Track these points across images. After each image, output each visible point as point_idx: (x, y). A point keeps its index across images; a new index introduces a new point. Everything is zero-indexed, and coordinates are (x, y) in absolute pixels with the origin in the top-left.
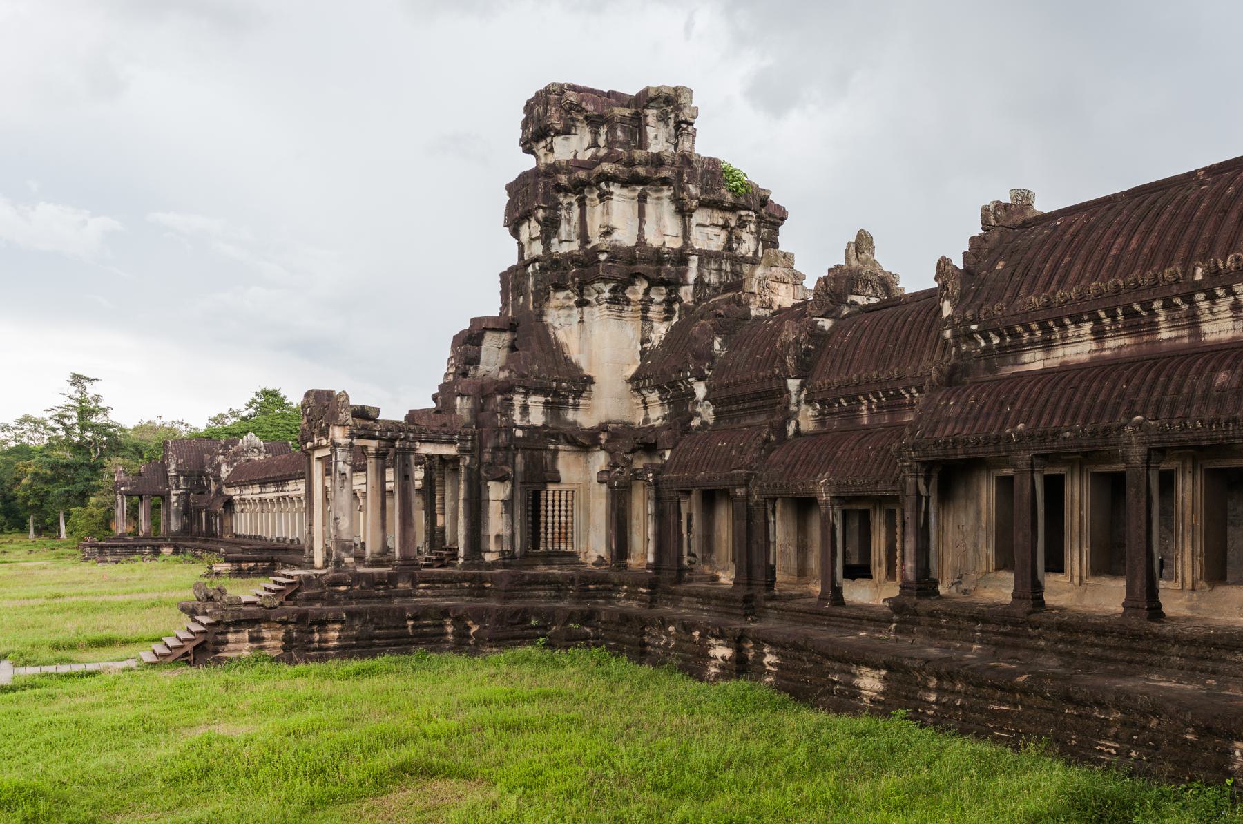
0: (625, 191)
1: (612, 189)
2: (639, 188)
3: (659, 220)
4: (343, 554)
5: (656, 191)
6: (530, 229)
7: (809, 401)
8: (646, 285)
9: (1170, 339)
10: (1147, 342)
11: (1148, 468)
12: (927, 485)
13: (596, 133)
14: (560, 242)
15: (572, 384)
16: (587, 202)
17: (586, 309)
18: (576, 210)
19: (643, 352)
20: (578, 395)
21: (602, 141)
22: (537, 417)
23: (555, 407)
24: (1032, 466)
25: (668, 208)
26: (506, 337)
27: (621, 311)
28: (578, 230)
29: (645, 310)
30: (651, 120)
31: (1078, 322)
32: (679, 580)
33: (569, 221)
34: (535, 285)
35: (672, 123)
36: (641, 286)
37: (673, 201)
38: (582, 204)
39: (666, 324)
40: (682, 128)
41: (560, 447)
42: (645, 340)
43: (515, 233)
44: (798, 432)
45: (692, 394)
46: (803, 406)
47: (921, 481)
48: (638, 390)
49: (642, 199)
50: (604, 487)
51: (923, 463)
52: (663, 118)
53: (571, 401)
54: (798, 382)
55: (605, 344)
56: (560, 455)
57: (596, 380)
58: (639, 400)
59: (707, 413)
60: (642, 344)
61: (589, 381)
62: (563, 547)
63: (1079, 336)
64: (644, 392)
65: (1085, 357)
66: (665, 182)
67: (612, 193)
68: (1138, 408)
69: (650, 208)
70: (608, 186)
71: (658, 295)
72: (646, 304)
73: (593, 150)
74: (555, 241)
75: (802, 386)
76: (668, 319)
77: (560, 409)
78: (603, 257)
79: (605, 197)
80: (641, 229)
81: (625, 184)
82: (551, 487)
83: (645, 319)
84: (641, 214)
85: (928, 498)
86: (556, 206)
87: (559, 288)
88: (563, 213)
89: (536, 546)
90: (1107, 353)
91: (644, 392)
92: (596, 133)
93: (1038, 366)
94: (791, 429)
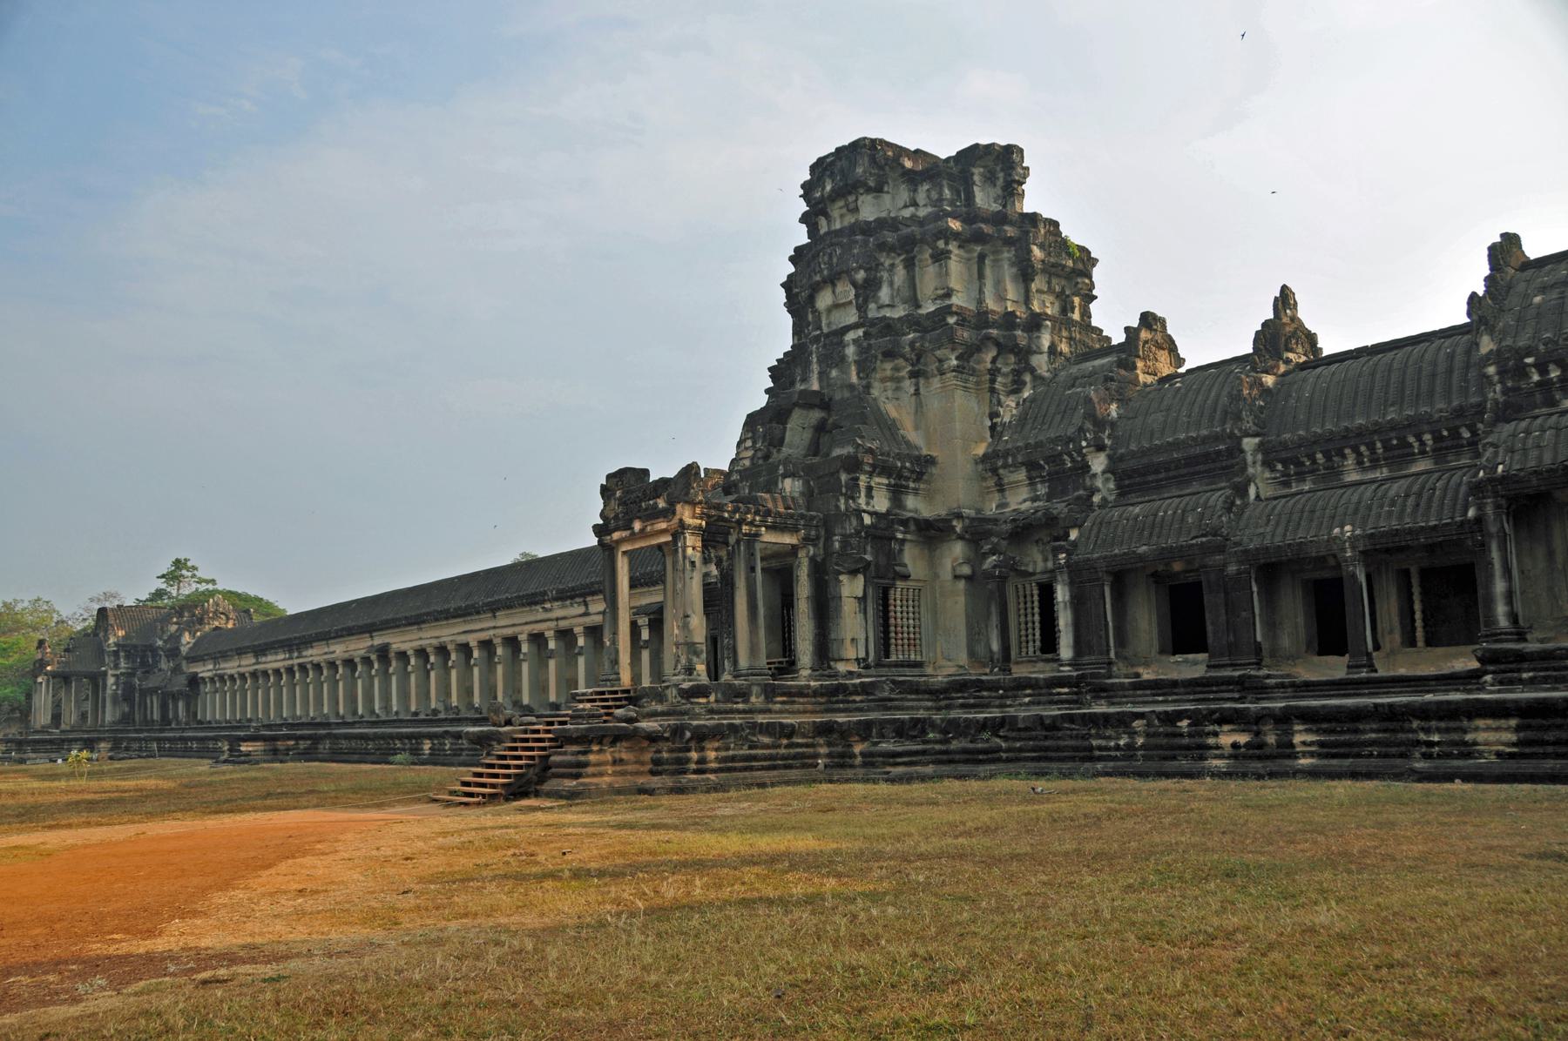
0: (961, 252)
1: (950, 247)
2: (979, 249)
3: (998, 283)
4: (695, 659)
5: (994, 253)
8: (992, 353)
14: (881, 307)
15: (911, 470)
17: (922, 381)
19: (993, 428)
20: (919, 477)
21: (921, 197)
23: (897, 493)
25: (1008, 272)
26: (816, 415)
27: (966, 381)
28: (906, 293)
29: (993, 381)
30: (976, 178)
33: (891, 284)
35: (1000, 182)
36: (989, 355)
37: (1012, 265)
38: (910, 264)
39: (1012, 397)
41: (909, 537)
42: (993, 415)
48: (994, 471)
49: (982, 258)
50: (961, 584)
52: (990, 179)
55: (948, 422)
56: (907, 547)
57: (940, 460)
58: (991, 483)
61: (931, 461)
64: (1001, 471)
66: (1009, 242)
67: (950, 252)
69: (988, 272)
70: (947, 244)
71: (1008, 364)
72: (994, 373)
73: (912, 209)
74: (872, 306)
78: (951, 320)
79: (940, 257)
80: (981, 291)
81: (964, 241)
82: (900, 584)
83: (993, 391)
84: (981, 276)
86: (873, 267)
87: (889, 355)
88: (885, 275)
89: (887, 656)
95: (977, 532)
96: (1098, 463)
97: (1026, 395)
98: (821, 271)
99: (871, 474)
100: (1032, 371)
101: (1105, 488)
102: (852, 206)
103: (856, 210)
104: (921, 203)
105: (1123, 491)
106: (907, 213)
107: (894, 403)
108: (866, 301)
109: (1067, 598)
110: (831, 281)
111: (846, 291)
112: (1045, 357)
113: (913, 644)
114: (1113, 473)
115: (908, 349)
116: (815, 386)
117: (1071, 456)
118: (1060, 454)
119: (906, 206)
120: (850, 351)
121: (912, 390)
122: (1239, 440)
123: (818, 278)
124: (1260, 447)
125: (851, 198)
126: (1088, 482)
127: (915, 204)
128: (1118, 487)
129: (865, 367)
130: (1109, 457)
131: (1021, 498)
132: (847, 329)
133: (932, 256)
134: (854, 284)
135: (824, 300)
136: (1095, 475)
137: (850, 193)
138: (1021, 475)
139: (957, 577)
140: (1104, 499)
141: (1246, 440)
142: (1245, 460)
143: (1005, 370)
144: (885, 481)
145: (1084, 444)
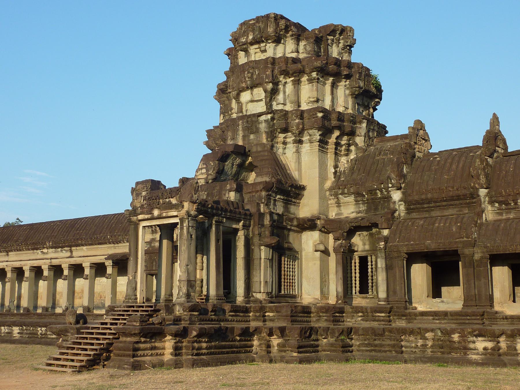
57: (308, 188)
60: (335, 169)
61: (303, 188)
71: (344, 141)
73: (296, 54)
74: (274, 103)
77: (289, 204)
86: (276, 84)
91: (340, 196)
95: (328, 227)
96: (396, 196)
97: (352, 156)
98: (246, 82)
99: (276, 193)
100: (356, 145)
101: (401, 209)
102: (263, 49)
103: (265, 51)
104: (301, 51)
105: (409, 210)
106: (294, 55)
107: (288, 155)
108: (271, 100)
109: (384, 266)
110: (252, 87)
111: (259, 93)
112: (362, 138)
113: (291, 285)
114: (405, 202)
115: (295, 128)
116: (240, 143)
117: (381, 192)
118: (376, 190)
119: (292, 52)
120: (263, 127)
121: (294, 150)
122: (477, 189)
123: (244, 85)
124: (488, 194)
125: (263, 45)
126: (392, 206)
127: (298, 52)
128: (407, 209)
129: (272, 135)
130: (403, 193)
131: (350, 211)
132: (260, 115)
133: (308, 80)
134: (265, 91)
135: (245, 96)
136: (395, 202)
137: (263, 42)
138: (352, 199)
139: (316, 251)
140: (399, 215)
141: (481, 190)
142: (481, 200)
143: (343, 142)
144: (282, 197)
145: (390, 185)
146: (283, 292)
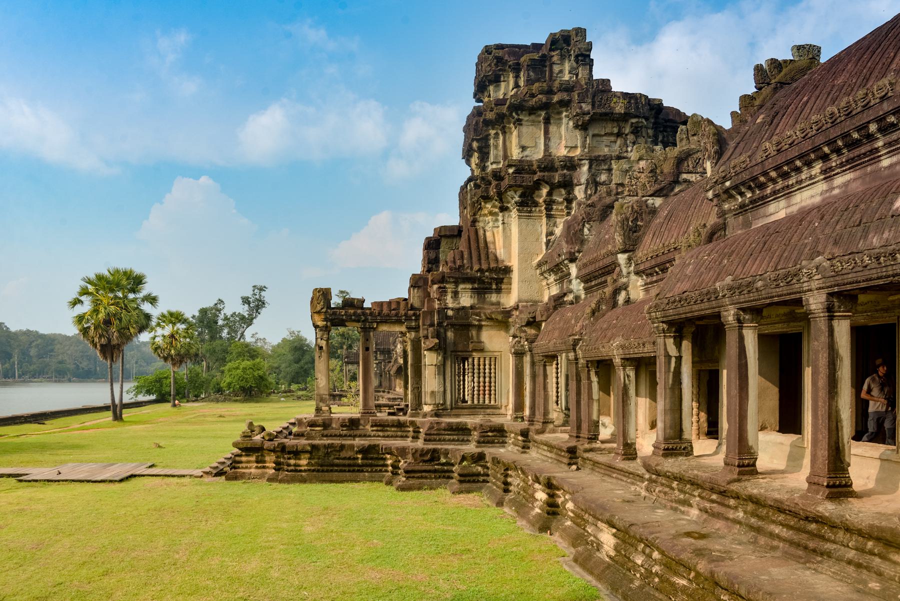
6: (475, 159)
7: (637, 273)
9: (891, 166)
10: (871, 172)
11: (831, 318)
12: (679, 346)
13: (517, 77)
16: (507, 130)
17: (506, 214)
18: (501, 137)
22: (466, 300)
24: (739, 321)
31: (809, 164)
32: (541, 432)
33: (496, 147)
34: (471, 198)
36: (545, 191)
40: (585, 59)
43: (468, 163)
44: (628, 301)
45: (569, 274)
46: (633, 277)
47: (670, 342)
51: (670, 323)
53: (494, 287)
54: (626, 256)
59: (577, 286)
60: (547, 237)
62: (487, 402)
63: (811, 178)
65: (818, 199)
68: (820, 248)
75: (629, 259)
76: (568, 214)
85: (679, 359)
87: (487, 198)
90: (836, 191)
92: (517, 77)
93: (782, 215)
94: (621, 298)
146: (469, 403)
